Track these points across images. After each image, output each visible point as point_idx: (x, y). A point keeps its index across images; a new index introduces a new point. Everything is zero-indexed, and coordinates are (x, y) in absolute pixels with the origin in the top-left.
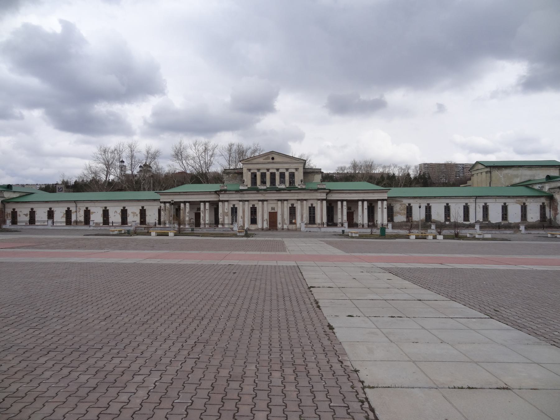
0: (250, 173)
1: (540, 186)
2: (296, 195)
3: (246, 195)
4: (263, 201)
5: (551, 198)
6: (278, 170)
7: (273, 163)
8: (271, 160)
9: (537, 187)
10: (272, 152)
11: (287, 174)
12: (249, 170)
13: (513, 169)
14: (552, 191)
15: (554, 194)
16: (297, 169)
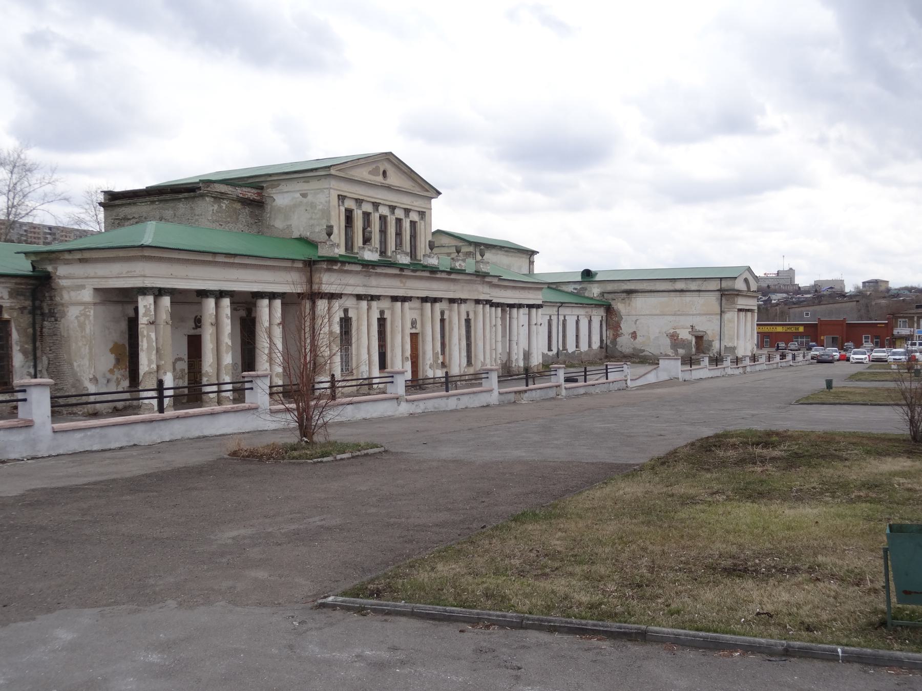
0: (343, 209)
1: (578, 287)
2: (452, 286)
3: (374, 281)
4: (404, 299)
5: (609, 309)
6: (393, 208)
7: (389, 188)
8: (380, 179)
9: (570, 288)
10: (389, 157)
11: (406, 225)
12: (342, 198)
13: (494, 251)
14: (610, 296)
15: (613, 303)
16: (422, 214)
